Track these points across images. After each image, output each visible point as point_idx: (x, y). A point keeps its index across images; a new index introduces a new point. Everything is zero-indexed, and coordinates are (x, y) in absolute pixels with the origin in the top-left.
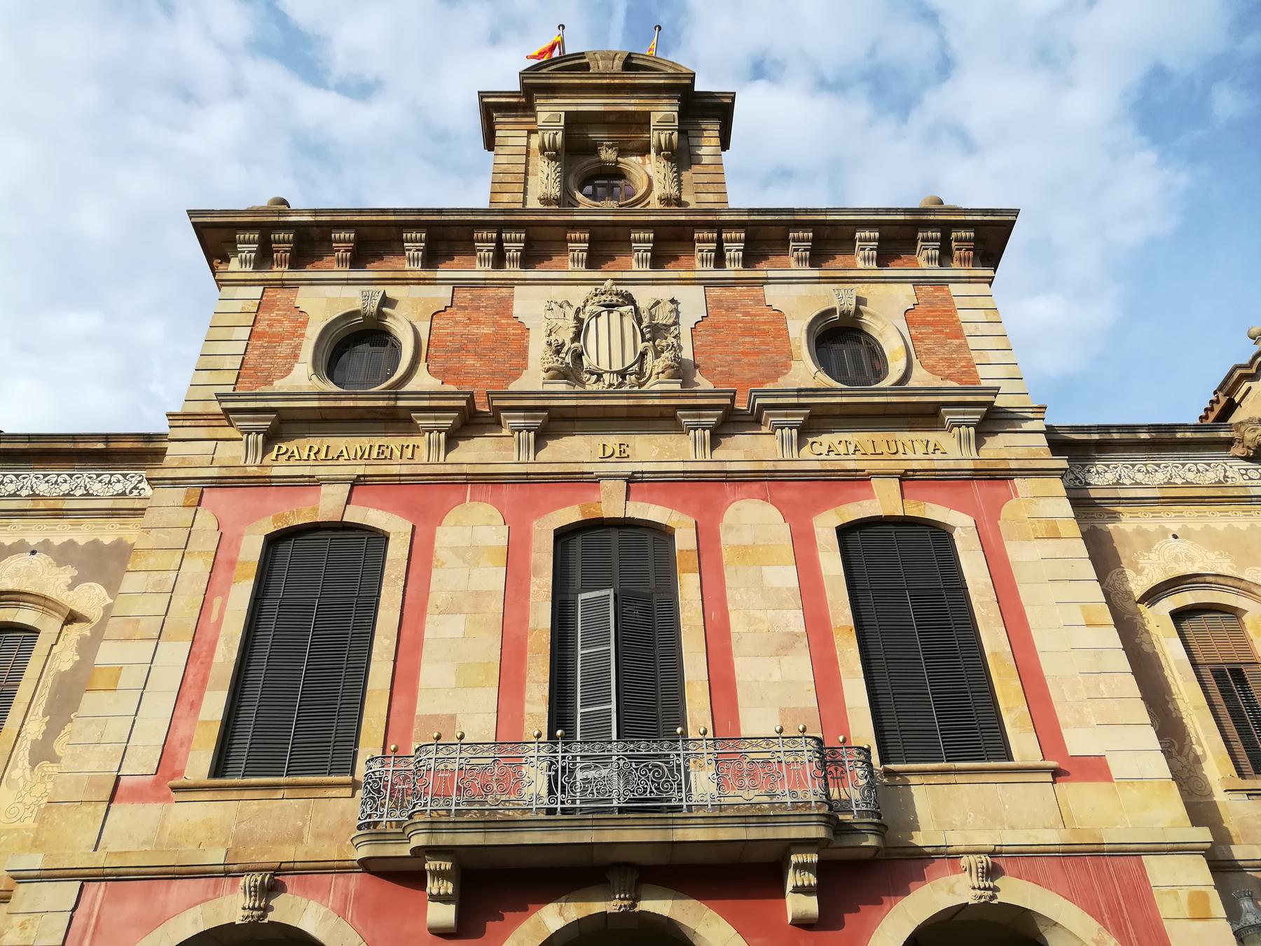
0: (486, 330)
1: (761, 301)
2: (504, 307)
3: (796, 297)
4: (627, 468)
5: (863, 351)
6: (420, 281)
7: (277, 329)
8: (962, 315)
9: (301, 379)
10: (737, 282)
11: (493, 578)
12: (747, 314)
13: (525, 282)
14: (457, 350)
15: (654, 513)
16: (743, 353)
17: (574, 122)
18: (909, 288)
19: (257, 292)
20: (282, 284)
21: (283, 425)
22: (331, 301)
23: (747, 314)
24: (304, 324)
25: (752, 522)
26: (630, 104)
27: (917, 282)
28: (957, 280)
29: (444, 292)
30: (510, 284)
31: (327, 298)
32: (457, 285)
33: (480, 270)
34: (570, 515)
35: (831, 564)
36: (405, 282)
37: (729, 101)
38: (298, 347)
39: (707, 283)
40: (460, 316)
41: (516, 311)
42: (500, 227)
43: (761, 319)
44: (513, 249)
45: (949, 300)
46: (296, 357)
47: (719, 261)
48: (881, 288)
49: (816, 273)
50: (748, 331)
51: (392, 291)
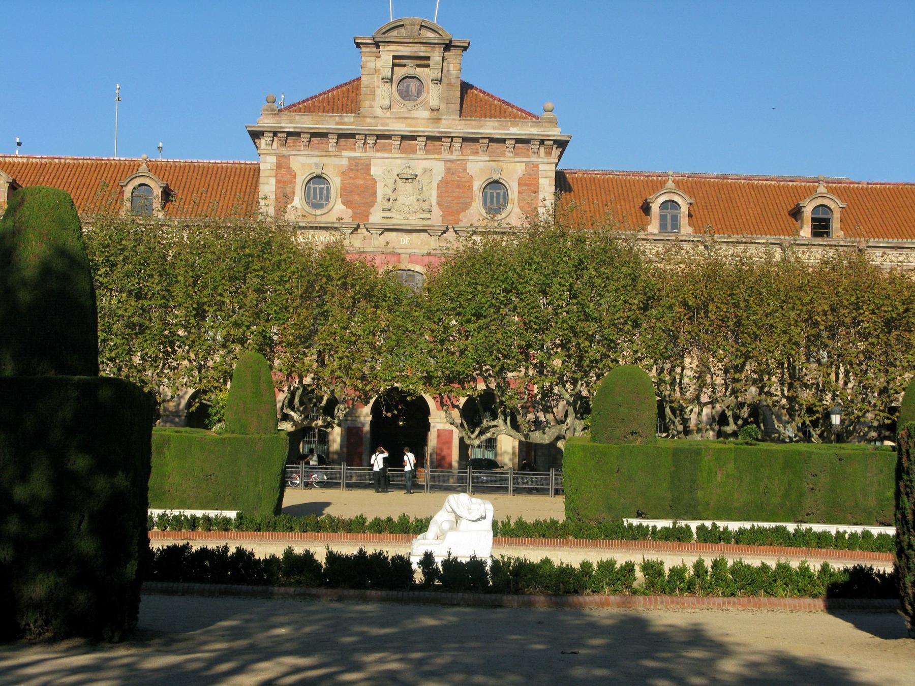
0: (361, 182)
1: (465, 170)
2: (368, 167)
3: (479, 167)
4: (409, 251)
5: (501, 192)
6: (336, 156)
7: (285, 179)
10: (457, 160)
12: (459, 177)
13: (375, 158)
14: (351, 192)
16: (456, 198)
18: (523, 166)
20: (283, 156)
22: (303, 165)
23: (459, 177)
24: (295, 177)
26: (422, 51)
27: (527, 164)
28: (543, 163)
29: (344, 162)
30: (370, 158)
32: (350, 159)
33: (358, 154)
36: (330, 156)
37: (466, 45)
38: (294, 188)
39: (446, 160)
40: (352, 175)
41: (372, 172)
42: (366, 135)
43: (464, 180)
45: (538, 173)
46: (294, 193)
48: (513, 165)
49: (488, 158)
50: (458, 187)
51: (326, 160)
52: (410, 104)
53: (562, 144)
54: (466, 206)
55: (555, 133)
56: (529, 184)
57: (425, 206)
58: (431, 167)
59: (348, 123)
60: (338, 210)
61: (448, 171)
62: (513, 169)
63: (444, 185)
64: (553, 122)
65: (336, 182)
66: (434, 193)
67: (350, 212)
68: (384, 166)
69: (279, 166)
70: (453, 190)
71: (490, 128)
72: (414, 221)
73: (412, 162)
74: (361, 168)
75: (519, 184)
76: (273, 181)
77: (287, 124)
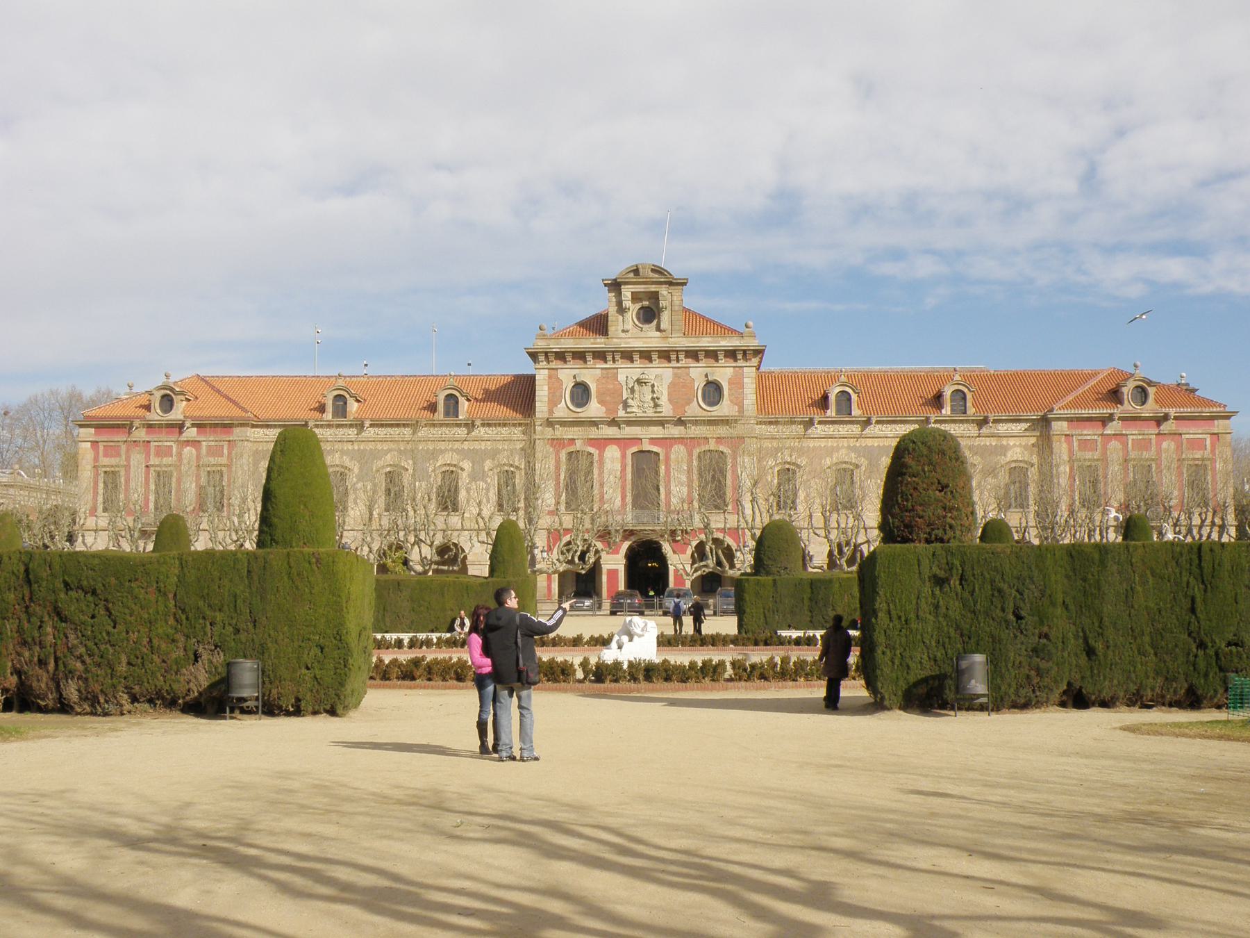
2: (616, 376)
3: (698, 373)
8: (745, 380)
9: (564, 409)
11: (618, 467)
15: (655, 449)
17: (636, 297)
19: (546, 371)
21: (563, 424)
25: (679, 451)
26: (653, 288)
31: (568, 374)
34: (635, 449)
35: (695, 463)
44: (617, 357)
47: (678, 360)
52: (646, 327)
53: (759, 352)
54: (689, 402)
55: (753, 343)
56: (737, 383)
57: (659, 402)
58: (661, 375)
59: (599, 343)
60: (594, 409)
61: (675, 375)
62: (723, 373)
63: (672, 386)
64: (753, 336)
65: (593, 388)
66: (665, 393)
67: (604, 409)
68: (627, 373)
69: (550, 377)
70: (679, 390)
71: (706, 342)
72: (650, 413)
73: (646, 371)
74: (611, 376)
75: (730, 383)
76: (546, 388)
77: (555, 346)
